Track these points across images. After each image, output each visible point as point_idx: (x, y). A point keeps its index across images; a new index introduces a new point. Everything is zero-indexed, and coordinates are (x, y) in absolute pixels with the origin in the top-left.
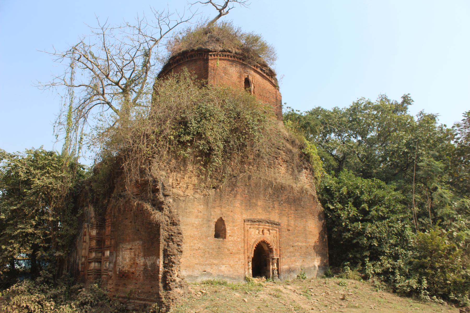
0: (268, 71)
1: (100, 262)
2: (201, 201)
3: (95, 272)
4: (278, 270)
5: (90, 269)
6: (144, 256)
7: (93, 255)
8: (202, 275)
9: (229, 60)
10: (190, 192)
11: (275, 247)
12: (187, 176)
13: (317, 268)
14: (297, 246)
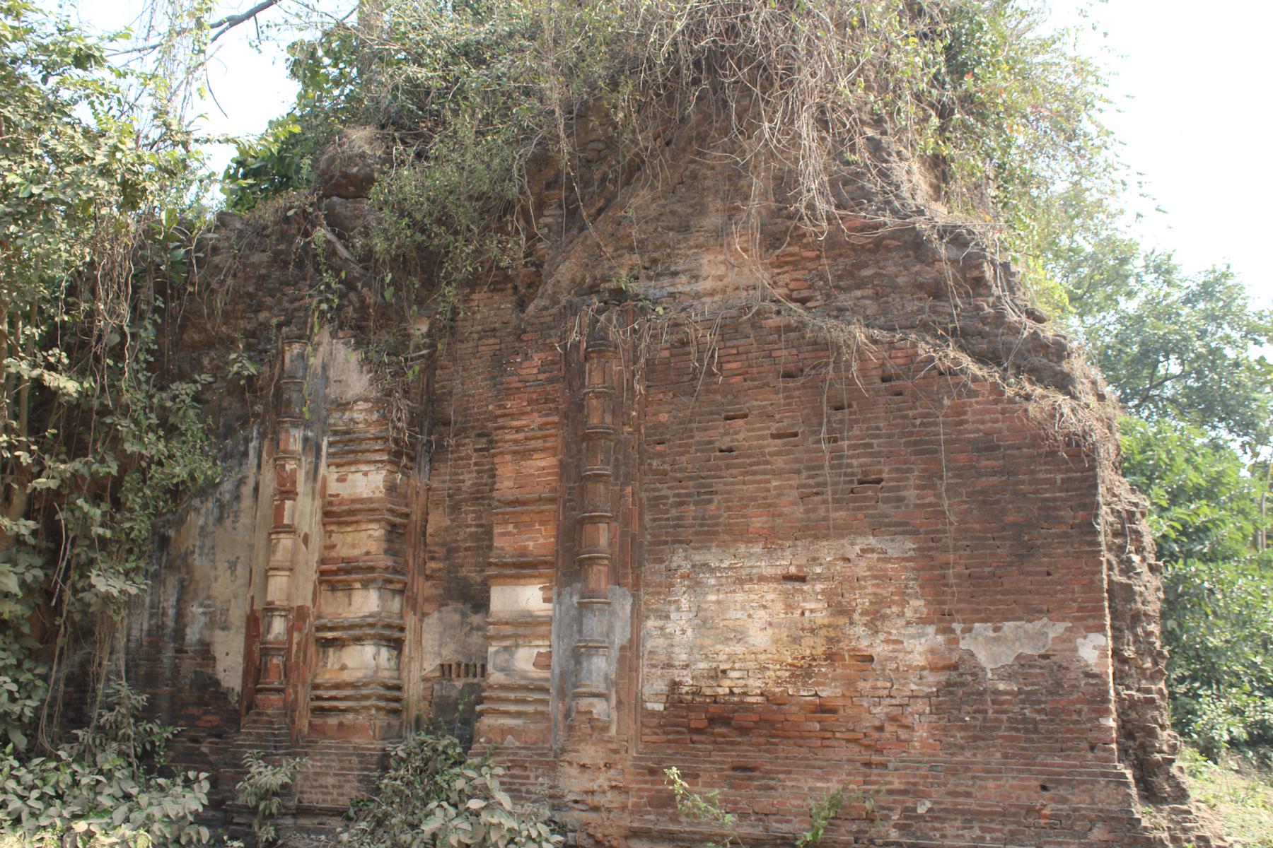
1: (396, 645)
3: (380, 698)
5: (327, 677)
6: (942, 618)
7: (367, 603)
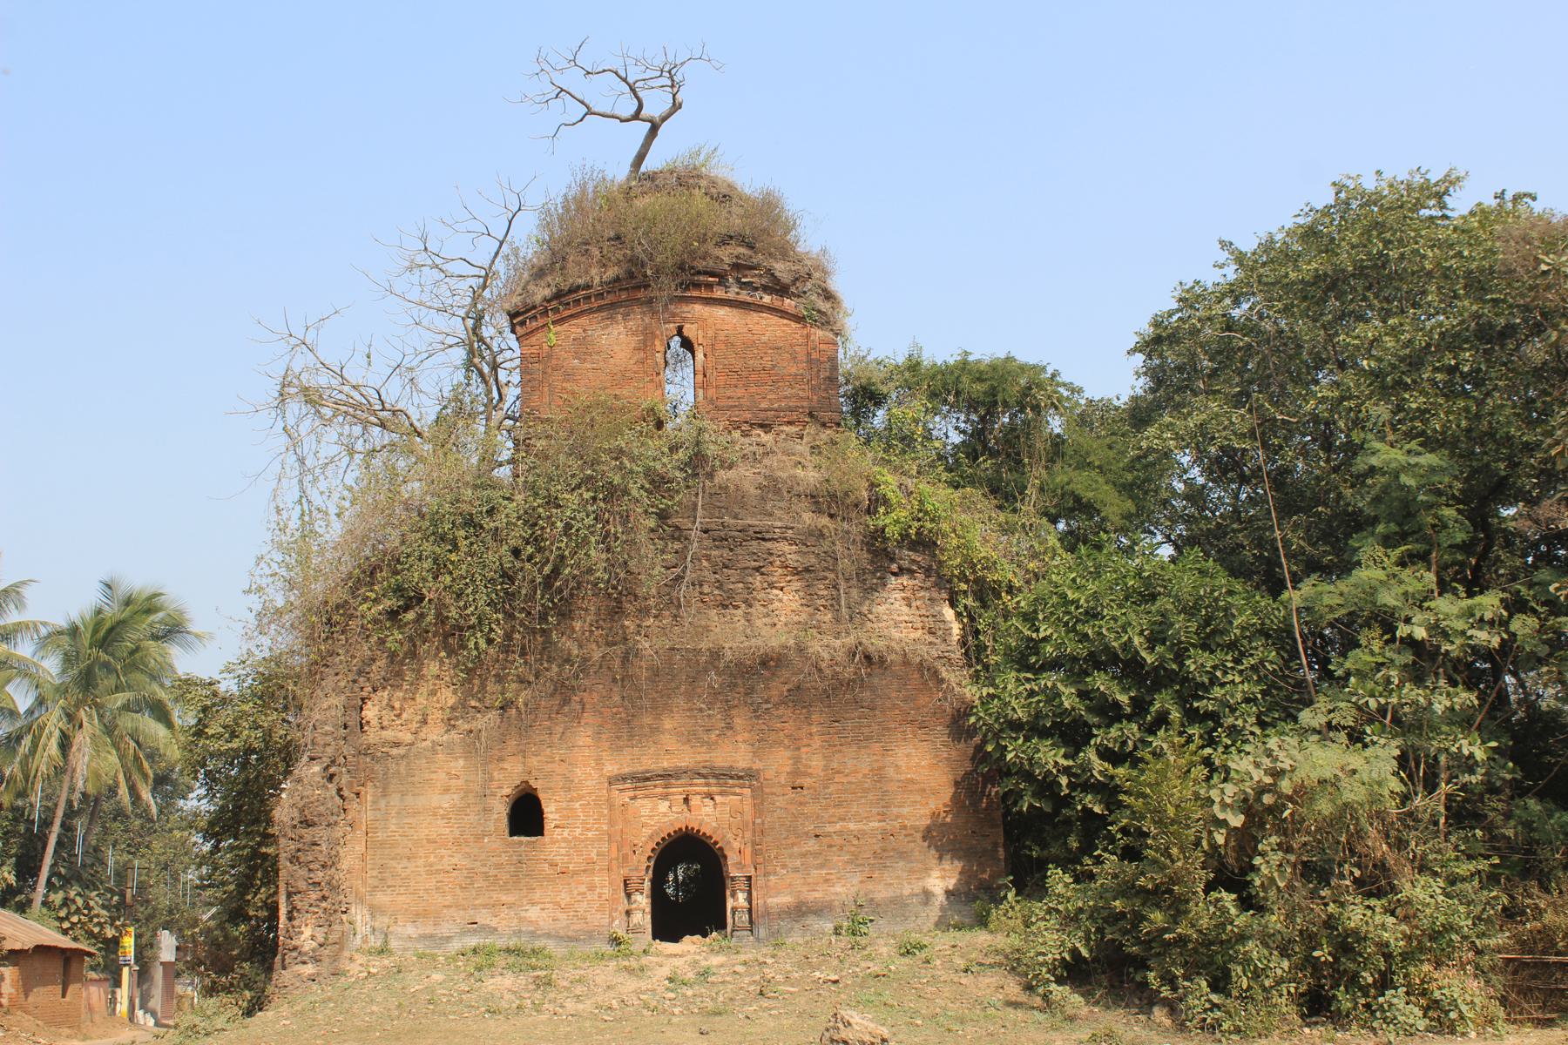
0: (764, 281)
2: (458, 750)
4: (750, 911)
8: (463, 933)
9: (591, 311)
10: (434, 733)
11: (736, 845)
12: (424, 690)
13: (941, 898)
14: (840, 833)
